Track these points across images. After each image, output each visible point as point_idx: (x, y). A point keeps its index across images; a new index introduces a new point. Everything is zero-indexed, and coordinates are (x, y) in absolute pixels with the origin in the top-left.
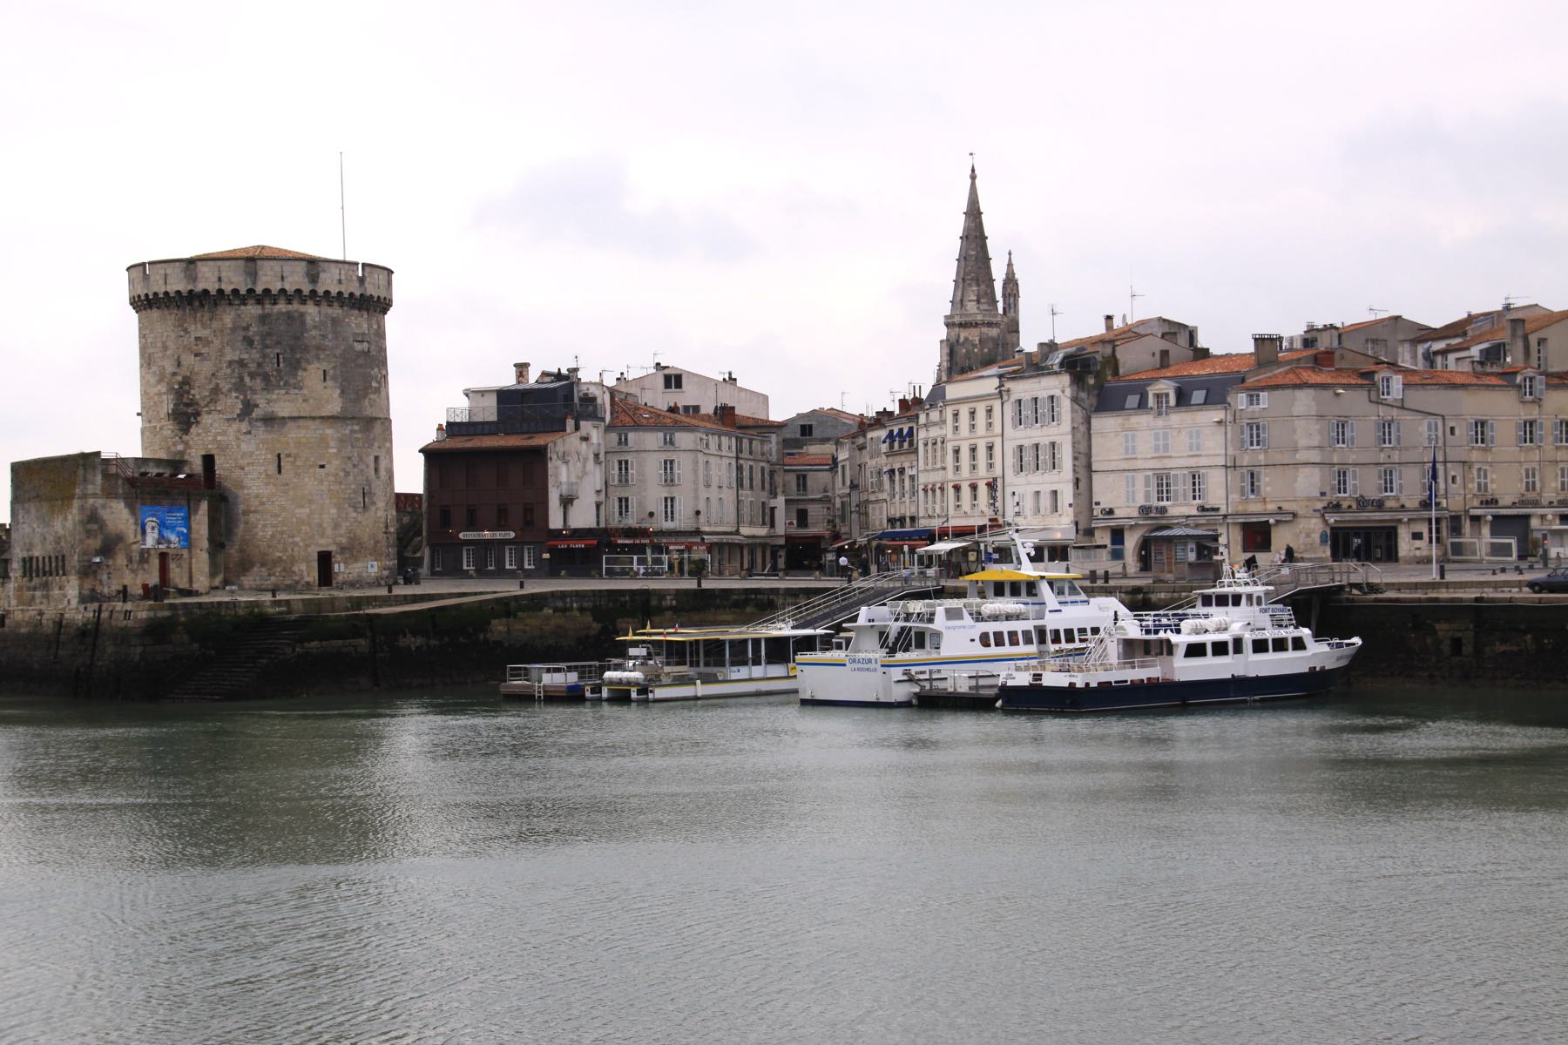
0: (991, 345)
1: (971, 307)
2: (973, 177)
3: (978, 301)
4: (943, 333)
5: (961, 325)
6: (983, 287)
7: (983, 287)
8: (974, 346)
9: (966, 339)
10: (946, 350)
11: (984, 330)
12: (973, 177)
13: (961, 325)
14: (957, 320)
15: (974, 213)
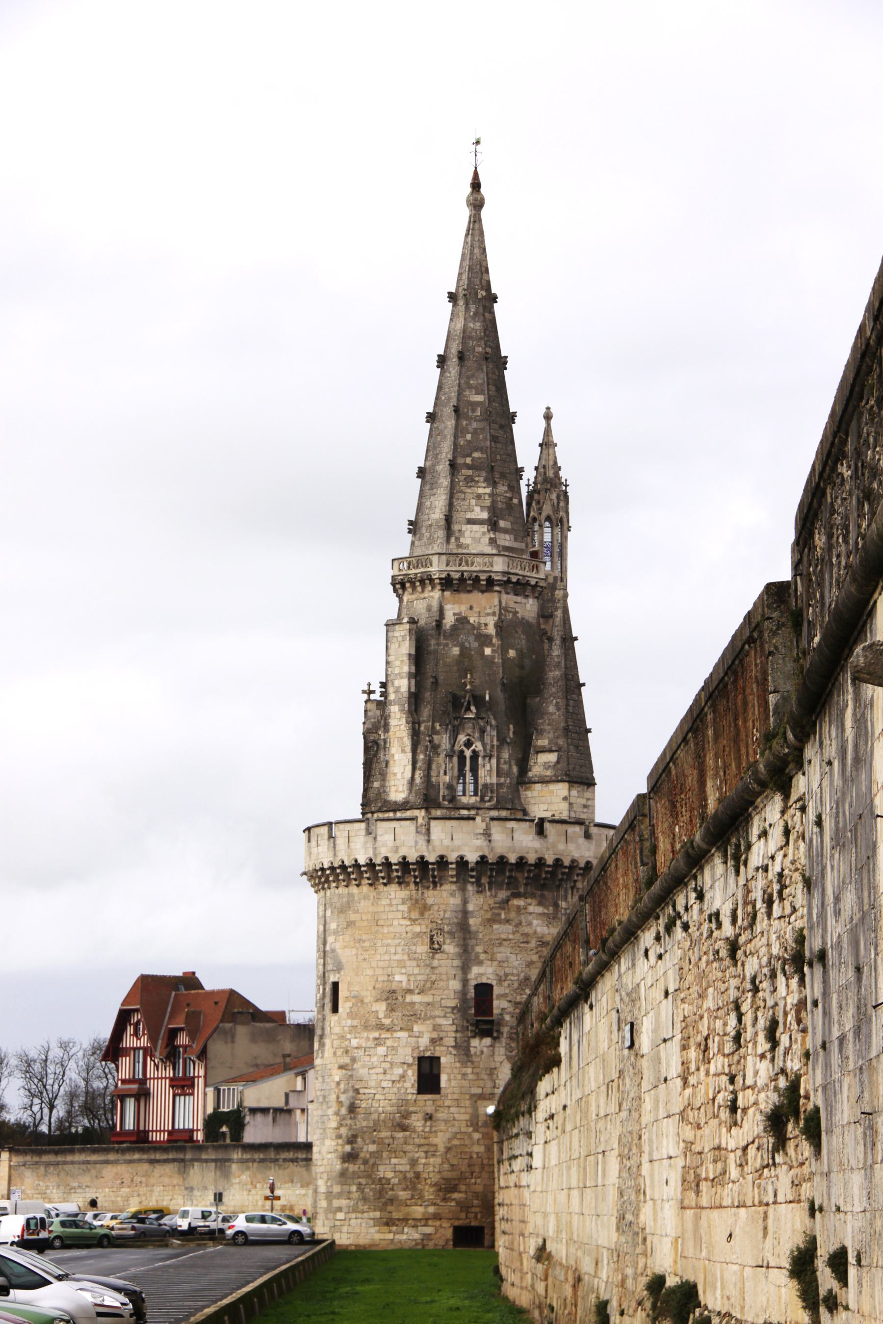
0: (522, 641)
1: (475, 538)
2: (476, 204)
3: (493, 525)
4: (389, 605)
5: (447, 583)
6: (502, 488)
7: (502, 488)
8: (484, 640)
9: (462, 620)
10: (404, 647)
11: (509, 599)
12: (476, 204)
13: (447, 583)
14: (437, 568)
15: (475, 295)
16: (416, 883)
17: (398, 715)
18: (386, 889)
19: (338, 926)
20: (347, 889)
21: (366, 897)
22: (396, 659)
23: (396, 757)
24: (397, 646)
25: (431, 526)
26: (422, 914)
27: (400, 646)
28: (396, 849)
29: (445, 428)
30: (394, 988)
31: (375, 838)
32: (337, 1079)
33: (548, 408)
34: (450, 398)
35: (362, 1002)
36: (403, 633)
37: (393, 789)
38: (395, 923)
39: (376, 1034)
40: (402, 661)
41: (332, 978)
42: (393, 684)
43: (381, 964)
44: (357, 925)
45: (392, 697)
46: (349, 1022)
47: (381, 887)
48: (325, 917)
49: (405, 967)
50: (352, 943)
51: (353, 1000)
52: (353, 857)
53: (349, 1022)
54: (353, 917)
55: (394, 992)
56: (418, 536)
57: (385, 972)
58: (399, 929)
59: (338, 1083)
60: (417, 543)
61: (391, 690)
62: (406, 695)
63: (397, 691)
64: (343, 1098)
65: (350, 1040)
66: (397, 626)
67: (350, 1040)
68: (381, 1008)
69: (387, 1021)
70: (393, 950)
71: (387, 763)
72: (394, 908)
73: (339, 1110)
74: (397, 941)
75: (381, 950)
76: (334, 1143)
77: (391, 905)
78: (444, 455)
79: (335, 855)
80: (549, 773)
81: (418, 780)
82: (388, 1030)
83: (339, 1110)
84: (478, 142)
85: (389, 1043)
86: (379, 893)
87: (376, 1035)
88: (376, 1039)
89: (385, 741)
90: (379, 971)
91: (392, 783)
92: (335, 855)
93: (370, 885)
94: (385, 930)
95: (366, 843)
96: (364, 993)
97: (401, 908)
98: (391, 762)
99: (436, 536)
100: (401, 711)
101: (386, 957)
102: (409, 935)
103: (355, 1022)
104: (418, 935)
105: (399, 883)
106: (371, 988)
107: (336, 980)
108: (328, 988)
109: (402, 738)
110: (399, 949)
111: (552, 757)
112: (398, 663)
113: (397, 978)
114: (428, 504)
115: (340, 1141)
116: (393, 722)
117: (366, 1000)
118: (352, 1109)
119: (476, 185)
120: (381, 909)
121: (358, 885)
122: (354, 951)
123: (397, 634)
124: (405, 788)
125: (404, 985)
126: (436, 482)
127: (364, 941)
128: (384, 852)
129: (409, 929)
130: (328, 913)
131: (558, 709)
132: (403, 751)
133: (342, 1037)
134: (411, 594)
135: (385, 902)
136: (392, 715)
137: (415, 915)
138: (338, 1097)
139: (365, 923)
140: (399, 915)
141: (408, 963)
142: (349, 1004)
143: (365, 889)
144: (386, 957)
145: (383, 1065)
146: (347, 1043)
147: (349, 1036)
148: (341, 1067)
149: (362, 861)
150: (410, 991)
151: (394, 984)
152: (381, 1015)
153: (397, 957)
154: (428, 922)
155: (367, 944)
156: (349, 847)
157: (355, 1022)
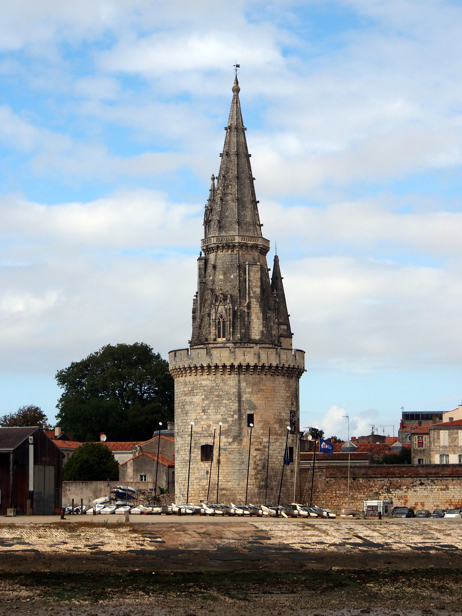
2: (236, 90)
12: (236, 90)
16: (287, 376)
17: (255, 303)
18: (278, 377)
19: (252, 391)
20: (258, 376)
21: (269, 380)
22: (254, 279)
23: (254, 320)
24: (254, 273)
25: (246, 223)
26: (289, 389)
27: (255, 274)
28: (287, 361)
29: (244, 183)
30: (282, 417)
31: (280, 356)
32: (255, 455)
33: (213, 175)
34: (244, 171)
35: (269, 423)
36: (257, 269)
37: (253, 334)
38: (281, 392)
39: (276, 437)
40: (257, 281)
41: (249, 412)
42: (252, 290)
43: (277, 408)
44: (265, 391)
45: (252, 295)
46: (262, 431)
47: (276, 376)
48: (239, 386)
49: (285, 410)
50: (263, 399)
51: (264, 422)
52: (270, 363)
53: (262, 431)
54: (262, 388)
55: (281, 420)
56: (240, 226)
57: (278, 411)
58: (282, 394)
59: (255, 456)
60: (240, 229)
61: (251, 292)
62: (259, 295)
63: (254, 293)
64: (259, 463)
65: (262, 439)
66: (254, 266)
67: (262, 439)
68: (277, 426)
69: (279, 432)
70: (281, 403)
71: (250, 322)
72: (281, 385)
73: (256, 467)
74: (282, 399)
75: (276, 402)
76: (254, 481)
77: (280, 384)
78: (246, 194)
79: (259, 361)
80: (285, 333)
81: (265, 332)
82: (280, 435)
83: (256, 467)
84: (238, 66)
85: (280, 441)
86: (275, 379)
87: (276, 437)
88: (275, 439)
89: (248, 313)
90: (276, 411)
91: (252, 331)
92: (259, 361)
93: (272, 375)
94: (278, 394)
95: (276, 357)
96: (270, 420)
97: (283, 385)
98: (252, 323)
99: (250, 228)
100: (257, 302)
101: (279, 405)
102: (286, 397)
103: (265, 432)
104: (288, 397)
105: (283, 376)
106: (273, 418)
107: (252, 413)
108: (245, 417)
109: (257, 313)
110: (283, 403)
111: (285, 327)
112: (255, 281)
113: (283, 414)
114: (242, 213)
115: (257, 480)
116: (253, 306)
117: (271, 423)
118: (265, 467)
119: (237, 83)
120: (276, 385)
121: (265, 375)
122: (264, 402)
123: (253, 269)
124: (260, 334)
125: (285, 418)
126: (245, 205)
127: (269, 398)
128: (283, 362)
129: (286, 394)
130: (243, 384)
131: (284, 308)
132: (258, 319)
133: (258, 438)
134: (244, 251)
135: (277, 382)
136: (252, 303)
137: (287, 389)
138: (255, 462)
139: (269, 391)
140: (282, 389)
141: (286, 409)
142: (261, 424)
143: (269, 376)
144: (279, 405)
145: (278, 450)
146: (261, 440)
147: (261, 437)
148: (256, 450)
149: (274, 364)
150: (286, 420)
151: (282, 417)
152: (277, 429)
153: (283, 406)
154: (290, 392)
155: (270, 399)
156: (268, 358)
157: (265, 432)
